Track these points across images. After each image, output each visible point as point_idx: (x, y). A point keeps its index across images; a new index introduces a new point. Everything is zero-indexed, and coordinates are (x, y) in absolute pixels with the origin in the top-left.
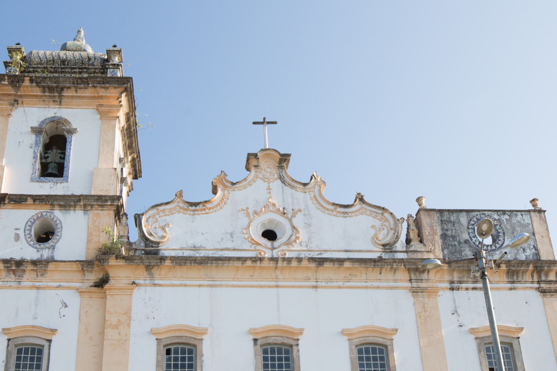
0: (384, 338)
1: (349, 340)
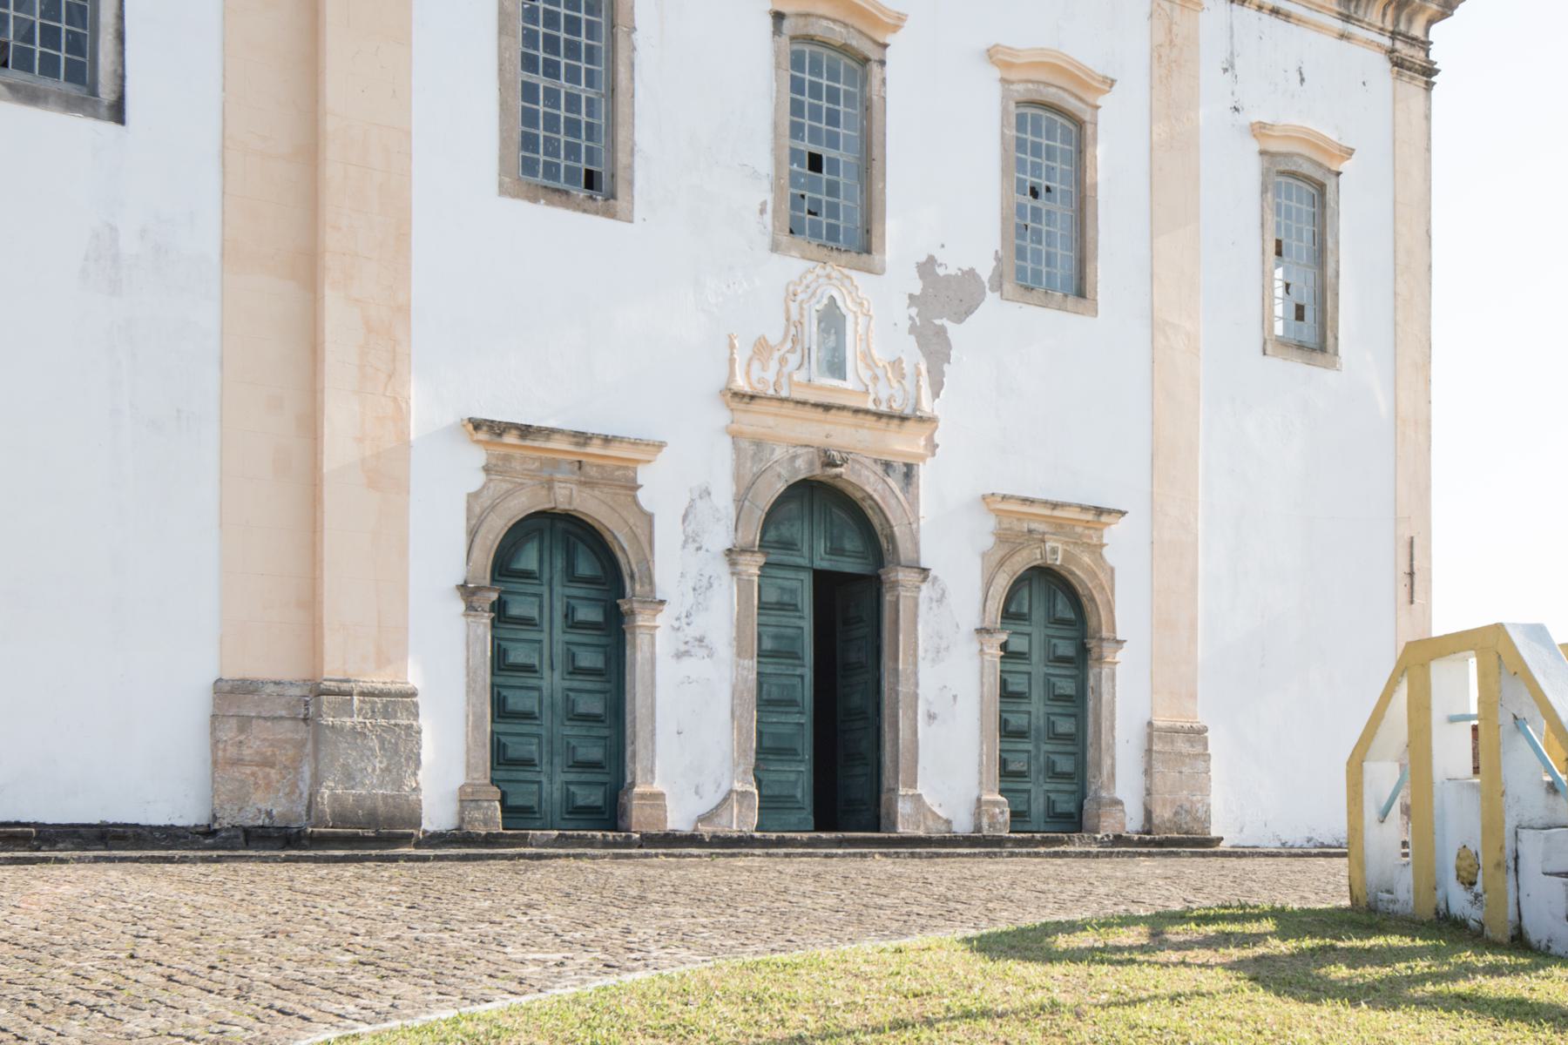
0: (1081, 100)
1: (1004, 81)
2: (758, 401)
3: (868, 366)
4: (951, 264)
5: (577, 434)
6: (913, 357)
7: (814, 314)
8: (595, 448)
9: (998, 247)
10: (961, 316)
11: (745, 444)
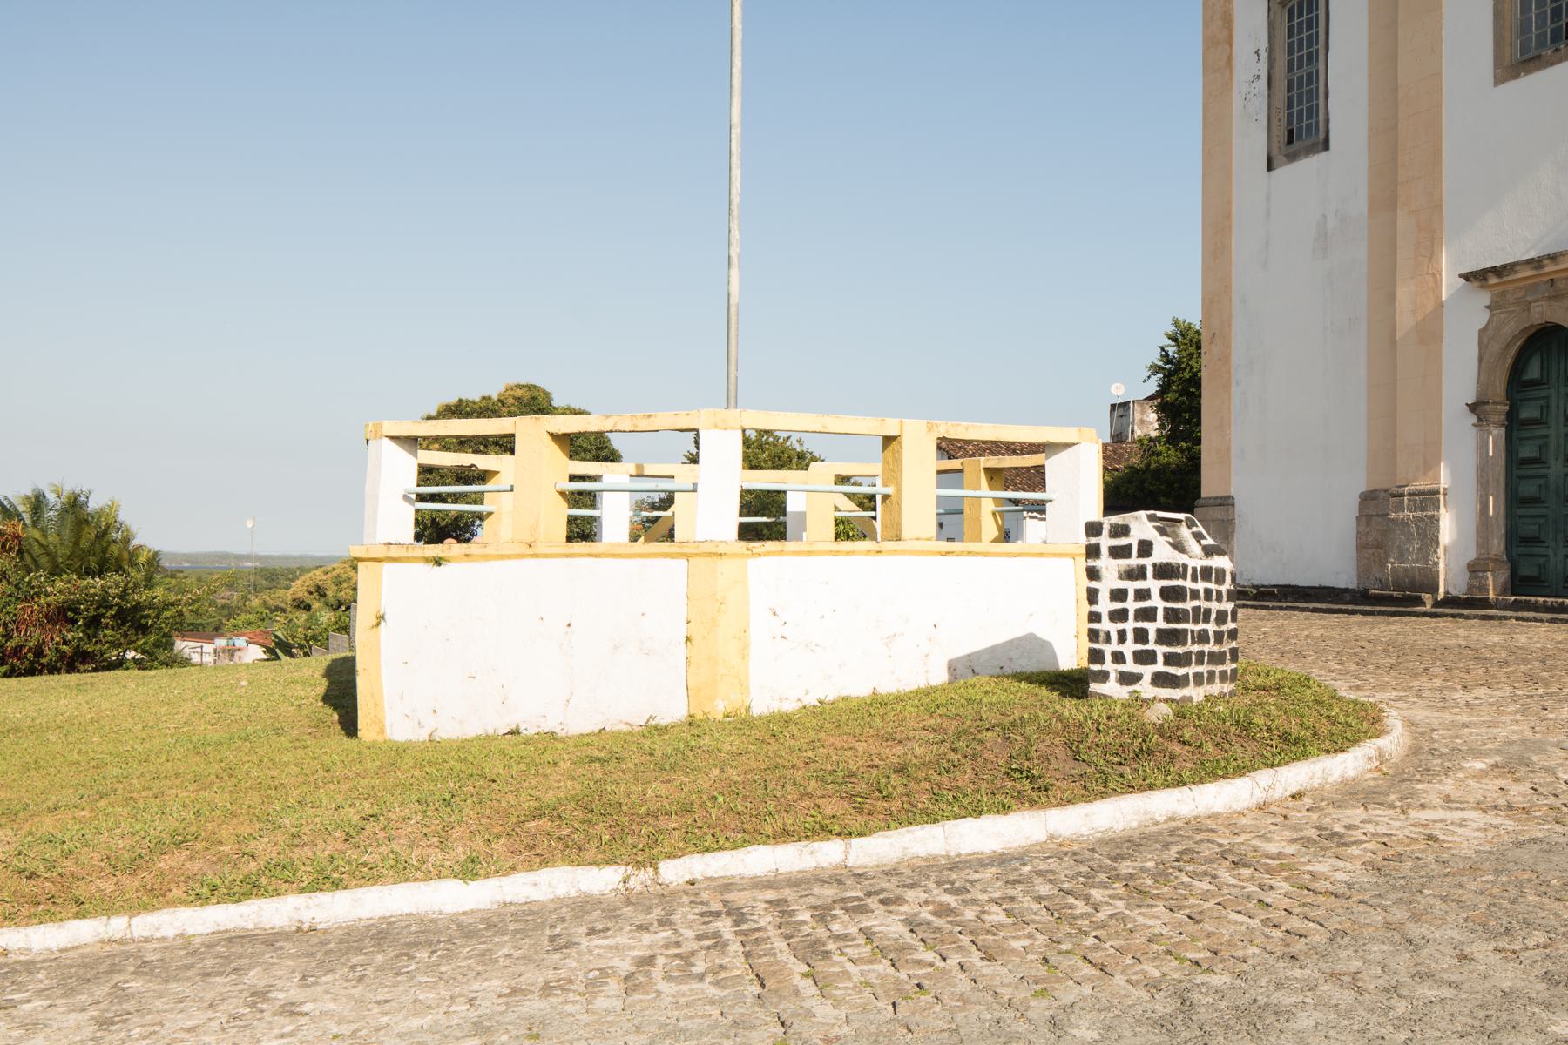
5: (1529, 261)
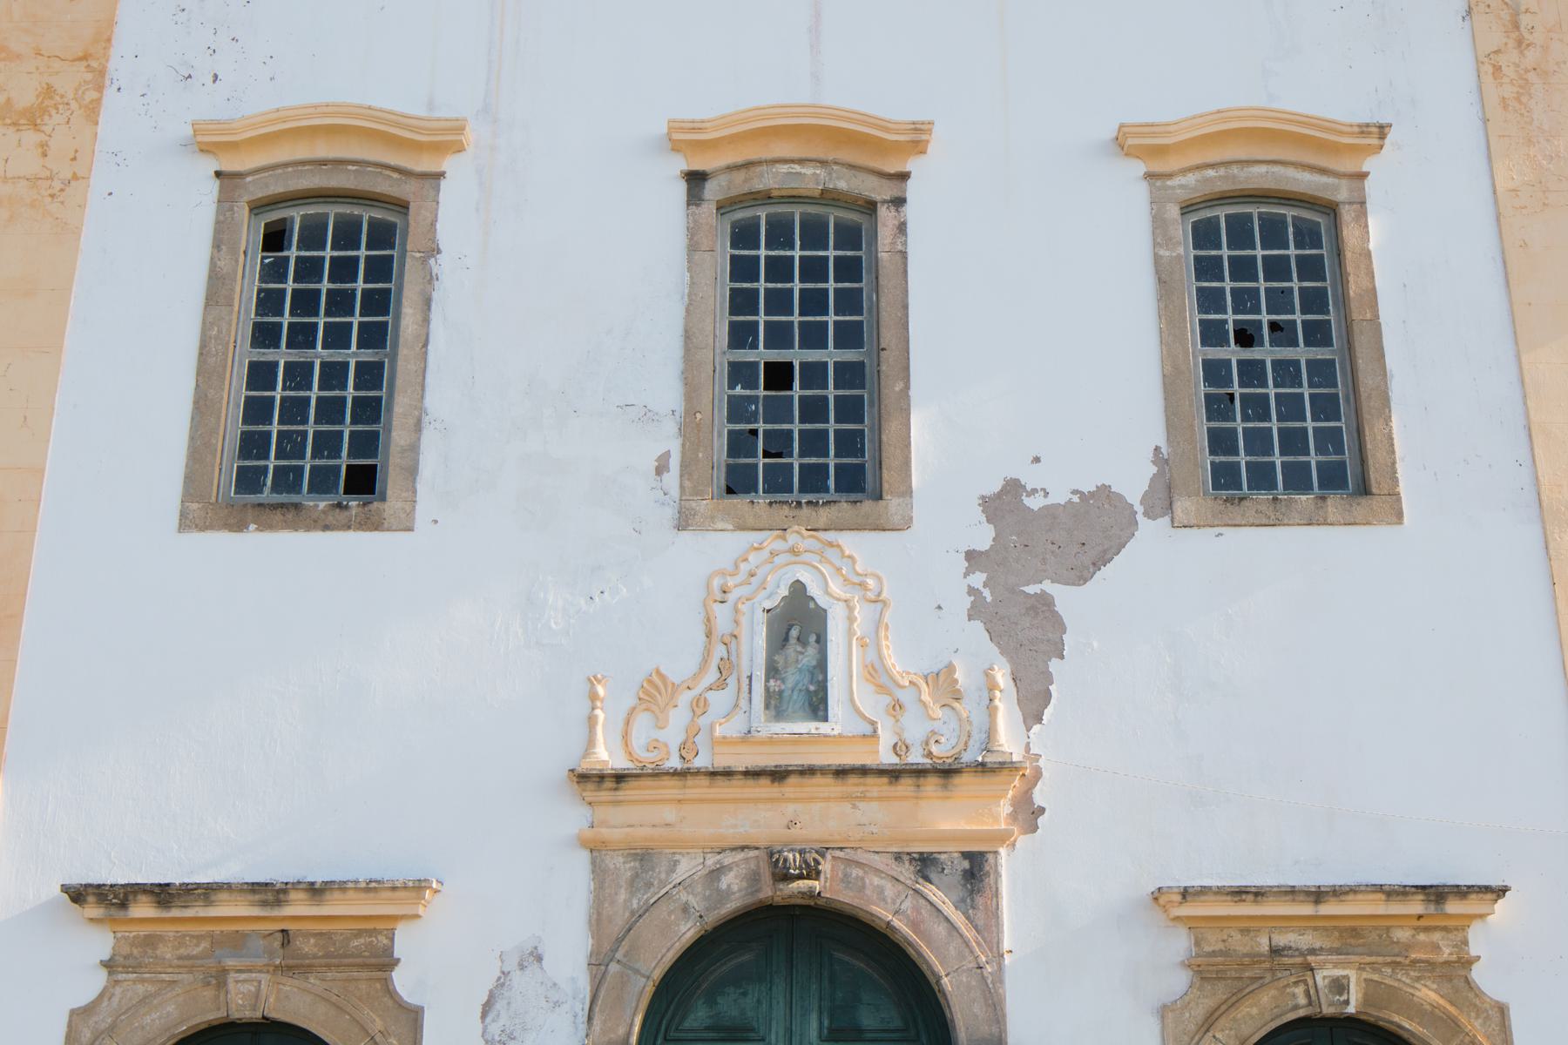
2: (633, 783)
3: (882, 689)
4: (1055, 485)
6: (977, 656)
7: (761, 618)
8: (298, 907)
9: (1160, 439)
10: (1080, 576)
11: (616, 861)
